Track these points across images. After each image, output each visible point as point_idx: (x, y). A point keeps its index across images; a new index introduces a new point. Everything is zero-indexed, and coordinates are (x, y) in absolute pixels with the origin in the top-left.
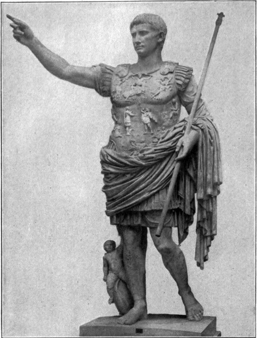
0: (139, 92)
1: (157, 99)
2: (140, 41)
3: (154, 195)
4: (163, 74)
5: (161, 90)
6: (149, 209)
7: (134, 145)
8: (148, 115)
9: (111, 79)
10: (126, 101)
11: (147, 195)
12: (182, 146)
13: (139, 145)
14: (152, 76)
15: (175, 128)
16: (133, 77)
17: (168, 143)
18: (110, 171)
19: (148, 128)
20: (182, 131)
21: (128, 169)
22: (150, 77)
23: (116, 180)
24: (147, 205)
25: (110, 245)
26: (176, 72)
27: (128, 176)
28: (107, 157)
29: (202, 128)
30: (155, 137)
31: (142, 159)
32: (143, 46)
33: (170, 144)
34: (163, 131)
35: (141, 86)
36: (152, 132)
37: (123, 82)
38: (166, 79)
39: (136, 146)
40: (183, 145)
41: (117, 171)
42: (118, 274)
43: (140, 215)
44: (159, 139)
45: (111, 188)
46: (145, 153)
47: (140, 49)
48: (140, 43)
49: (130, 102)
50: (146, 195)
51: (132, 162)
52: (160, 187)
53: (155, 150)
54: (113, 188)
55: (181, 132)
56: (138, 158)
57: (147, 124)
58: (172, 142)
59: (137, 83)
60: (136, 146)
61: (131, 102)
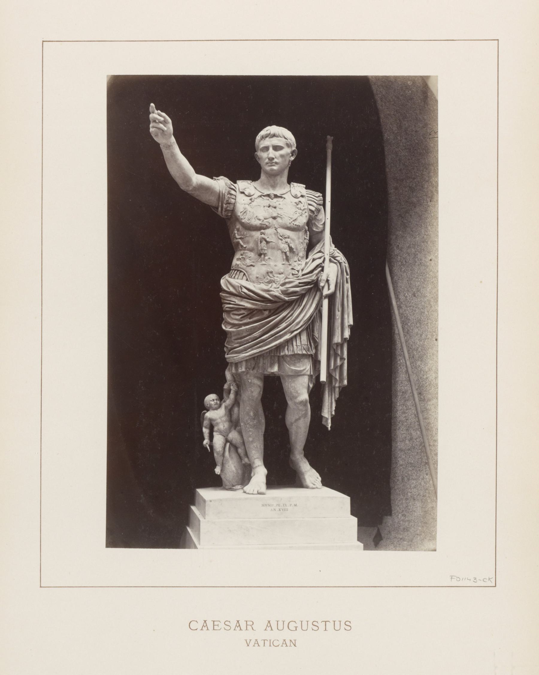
0: (276, 215)
1: (296, 225)
2: (274, 157)
3: (295, 336)
4: (296, 197)
5: (298, 214)
6: (290, 353)
7: (273, 277)
8: (286, 242)
9: (236, 196)
10: (261, 224)
11: (290, 335)
12: (328, 281)
13: (277, 277)
14: (284, 198)
15: (314, 260)
16: (262, 197)
17: (311, 277)
18: (244, 306)
19: (287, 257)
20: (321, 264)
21: (268, 304)
22: (283, 199)
23: (250, 319)
24: (288, 349)
25: (216, 400)
26: (307, 197)
27: (266, 313)
28: (241, 289)
29: (341, 261)
30: (293, 269)
31: (284, 293)
32: (276, 163)
33: (314, 278)
34: (300, 263)
35: (275, 208)
36: (290, 263)
37: (253, 202)
38: (300, 203)
39: (275, 278)
40: (328, 279)
41: (253, 307)
42: (227, 436)
43: (277, 359)
44: (298, 271)
45: (241, 327)
46: (288, 286)
47: (274, 166)
48: (273, 159)
49: (265, 225)
50: (288, 337)
51: (276, 296)
52: (302, 328)
53: (300, 283)
54: (243, 328)
55: (321, 265)
56: (280, 292)
57: (285, 253)
58: (315, 276)
59: (271, 204)
60: (275, 278)
61: (267, 226)
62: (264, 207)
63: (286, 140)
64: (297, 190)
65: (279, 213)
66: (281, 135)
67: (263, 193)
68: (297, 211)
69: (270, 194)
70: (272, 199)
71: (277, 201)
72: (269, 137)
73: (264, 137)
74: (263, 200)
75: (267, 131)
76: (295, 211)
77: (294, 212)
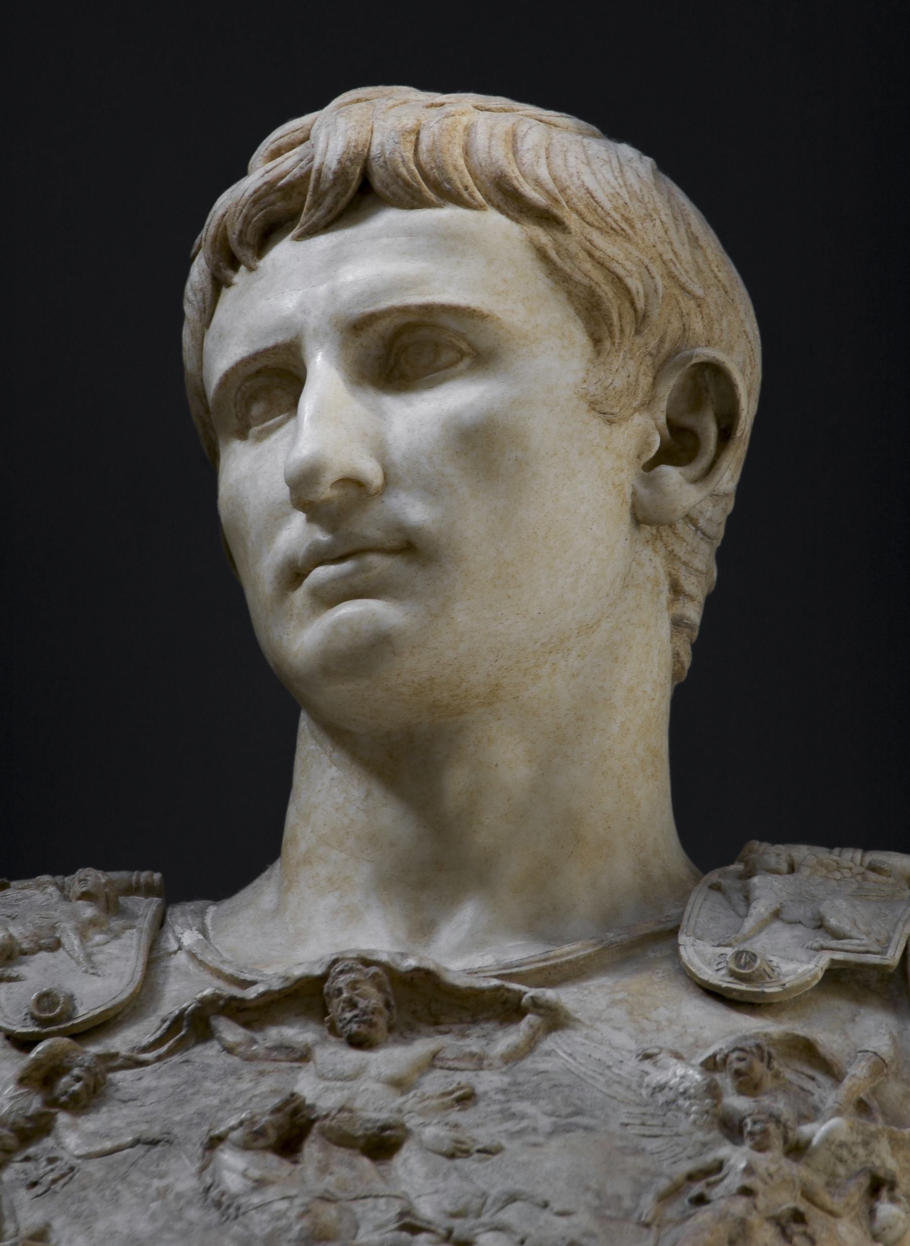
62: (214, 1142)
63: (542, 236)
64: (777, 915)
65: (426, 1209)
66: (462, 178)
67: (246, 984)
68: (719, 1166)
69: (324, 978)
70: (358, 1043)
71: (433, 1061)
72: (295, 232)
73: (233, 237)
74: (235, 1072)
75: (276, 153)
76: (687, 1167)
77: (663, 1184)
